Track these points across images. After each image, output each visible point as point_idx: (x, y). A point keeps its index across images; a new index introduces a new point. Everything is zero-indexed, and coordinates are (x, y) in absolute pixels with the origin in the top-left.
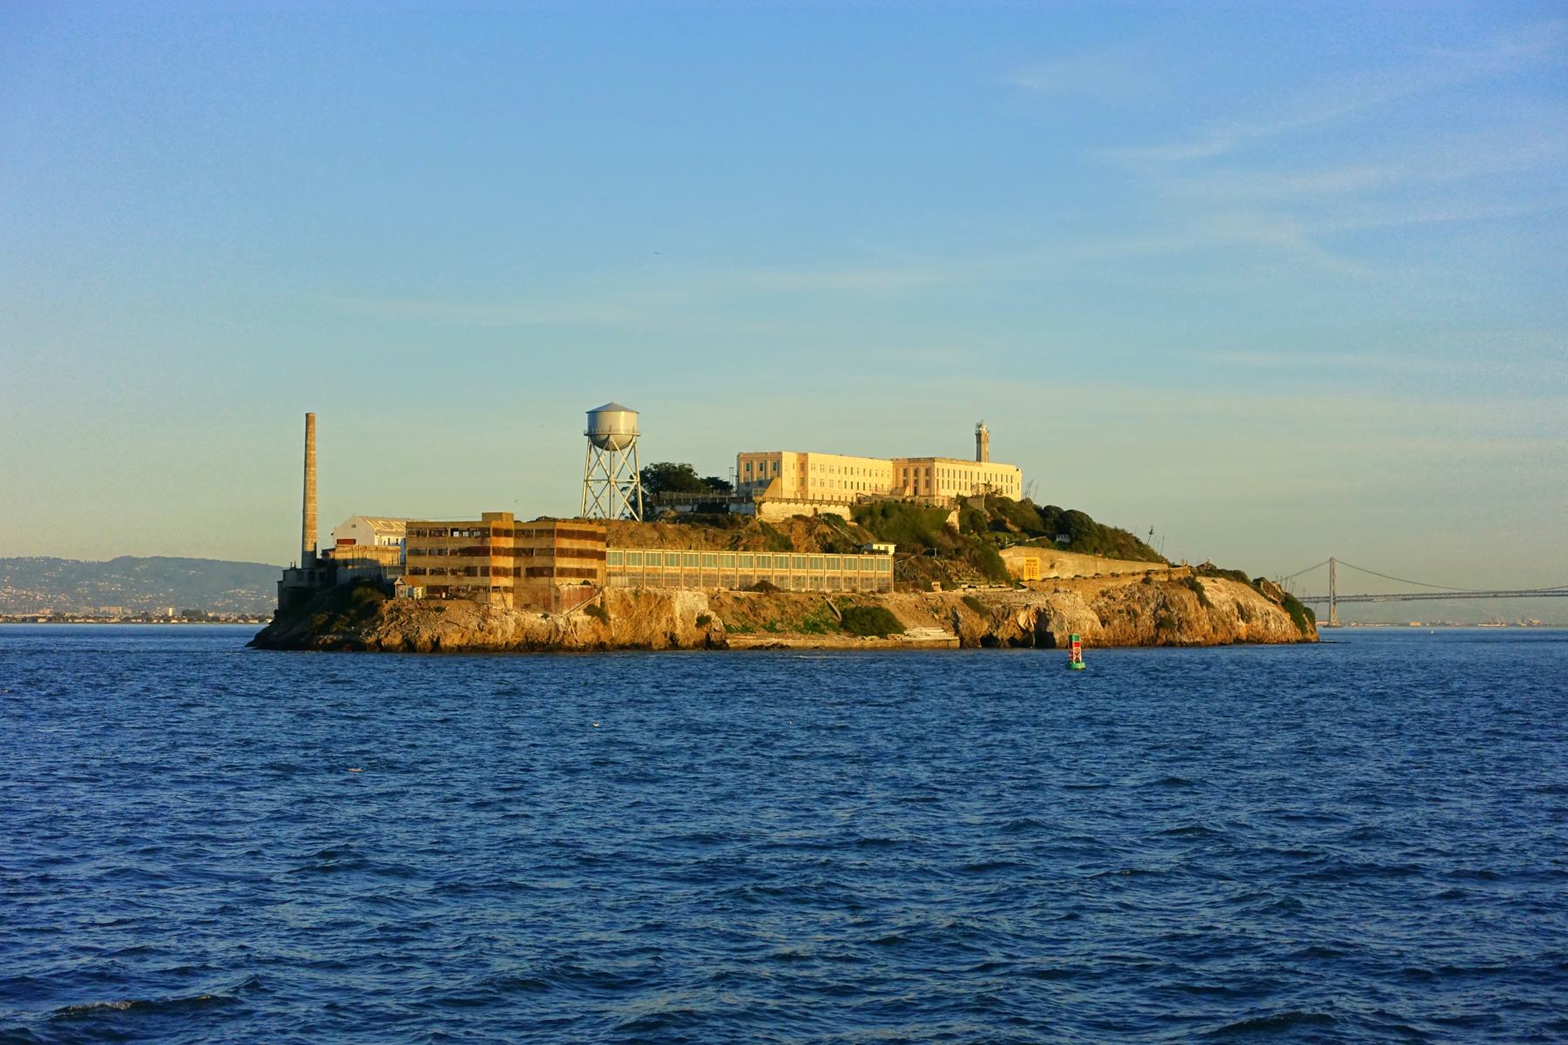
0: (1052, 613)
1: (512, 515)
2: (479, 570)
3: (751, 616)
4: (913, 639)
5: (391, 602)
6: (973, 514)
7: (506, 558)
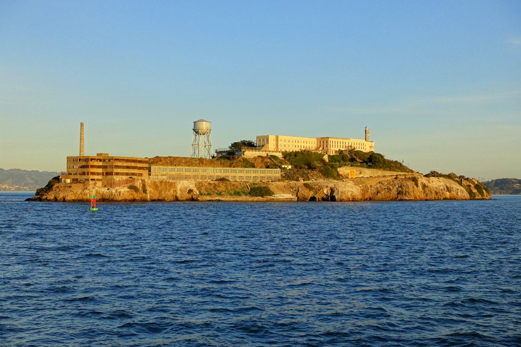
0: (335, 189)
1: (108, 154)
2: (86, 173)
3: (213, 190)
4: (276, 198)
5: (58, 184)
6: (343, 156)
7: (97, 169)
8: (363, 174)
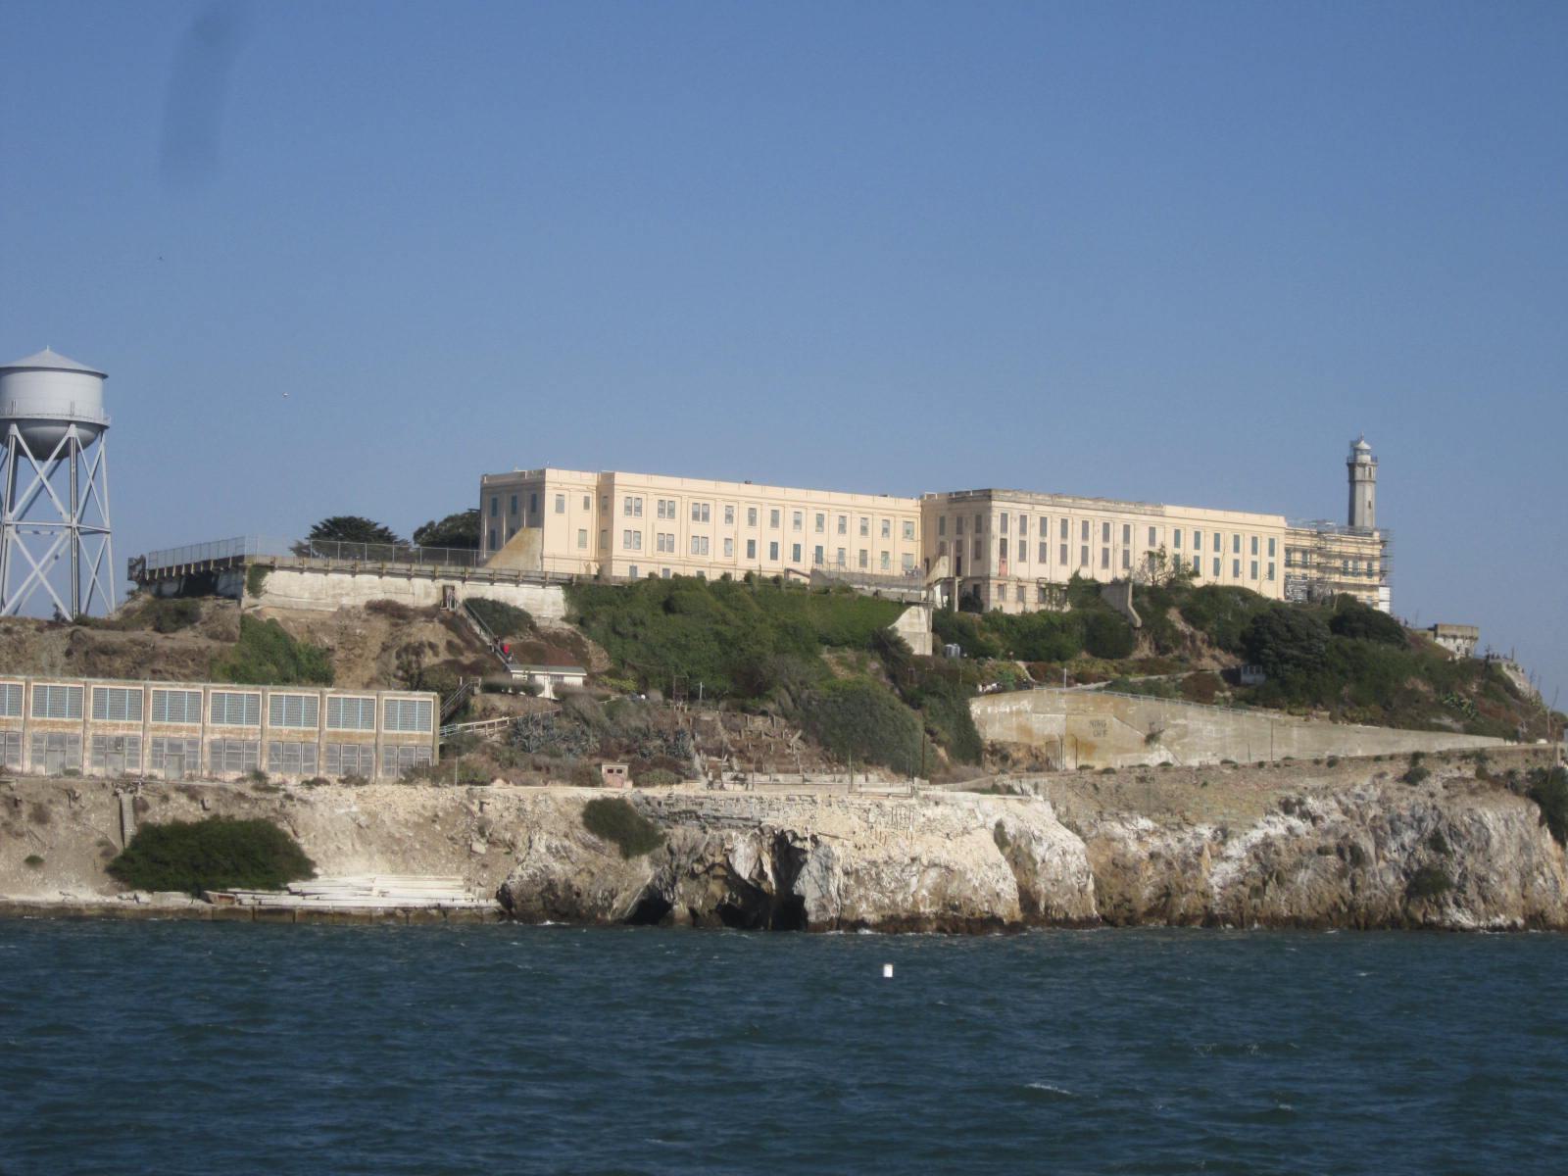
8: (1169, 747)
